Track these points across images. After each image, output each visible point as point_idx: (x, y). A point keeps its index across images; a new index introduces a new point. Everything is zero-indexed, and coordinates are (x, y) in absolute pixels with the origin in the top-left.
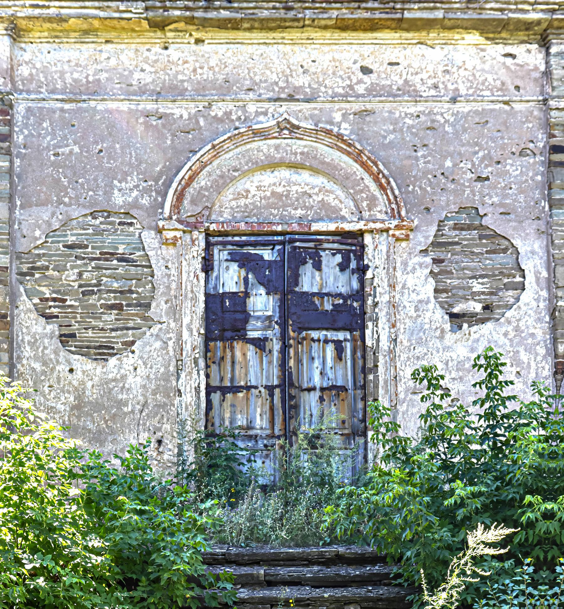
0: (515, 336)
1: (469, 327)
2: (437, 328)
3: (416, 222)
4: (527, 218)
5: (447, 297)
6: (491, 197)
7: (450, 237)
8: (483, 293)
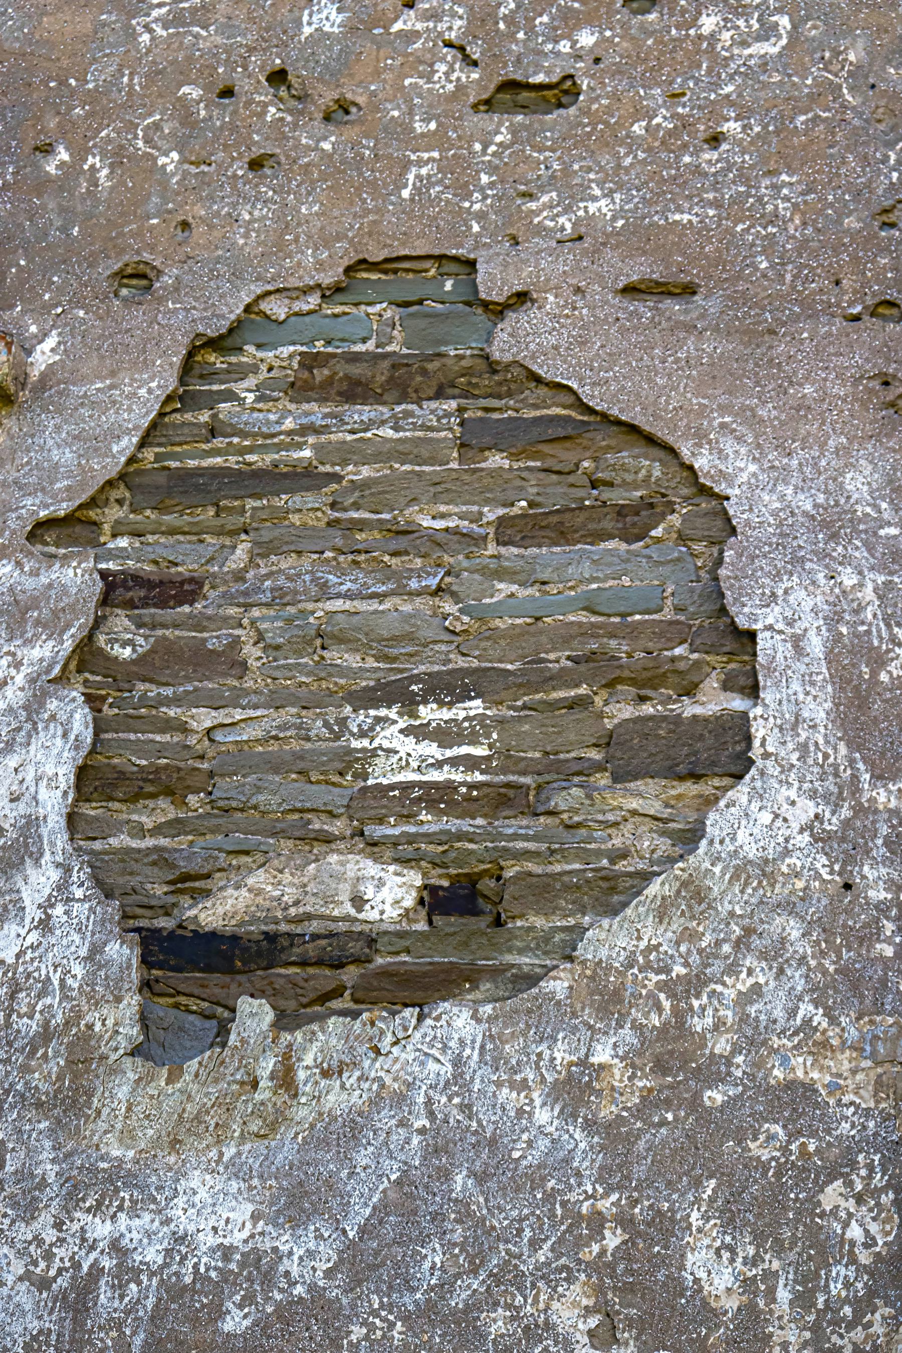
0: (650, 1102)
1: (285, 1021)
2: (46, 1035)
3: (44, 355)
4: (810, 310)
5: (175, 827)
6: (573, 194)
7: (266, 439)
8: (438, 796)
